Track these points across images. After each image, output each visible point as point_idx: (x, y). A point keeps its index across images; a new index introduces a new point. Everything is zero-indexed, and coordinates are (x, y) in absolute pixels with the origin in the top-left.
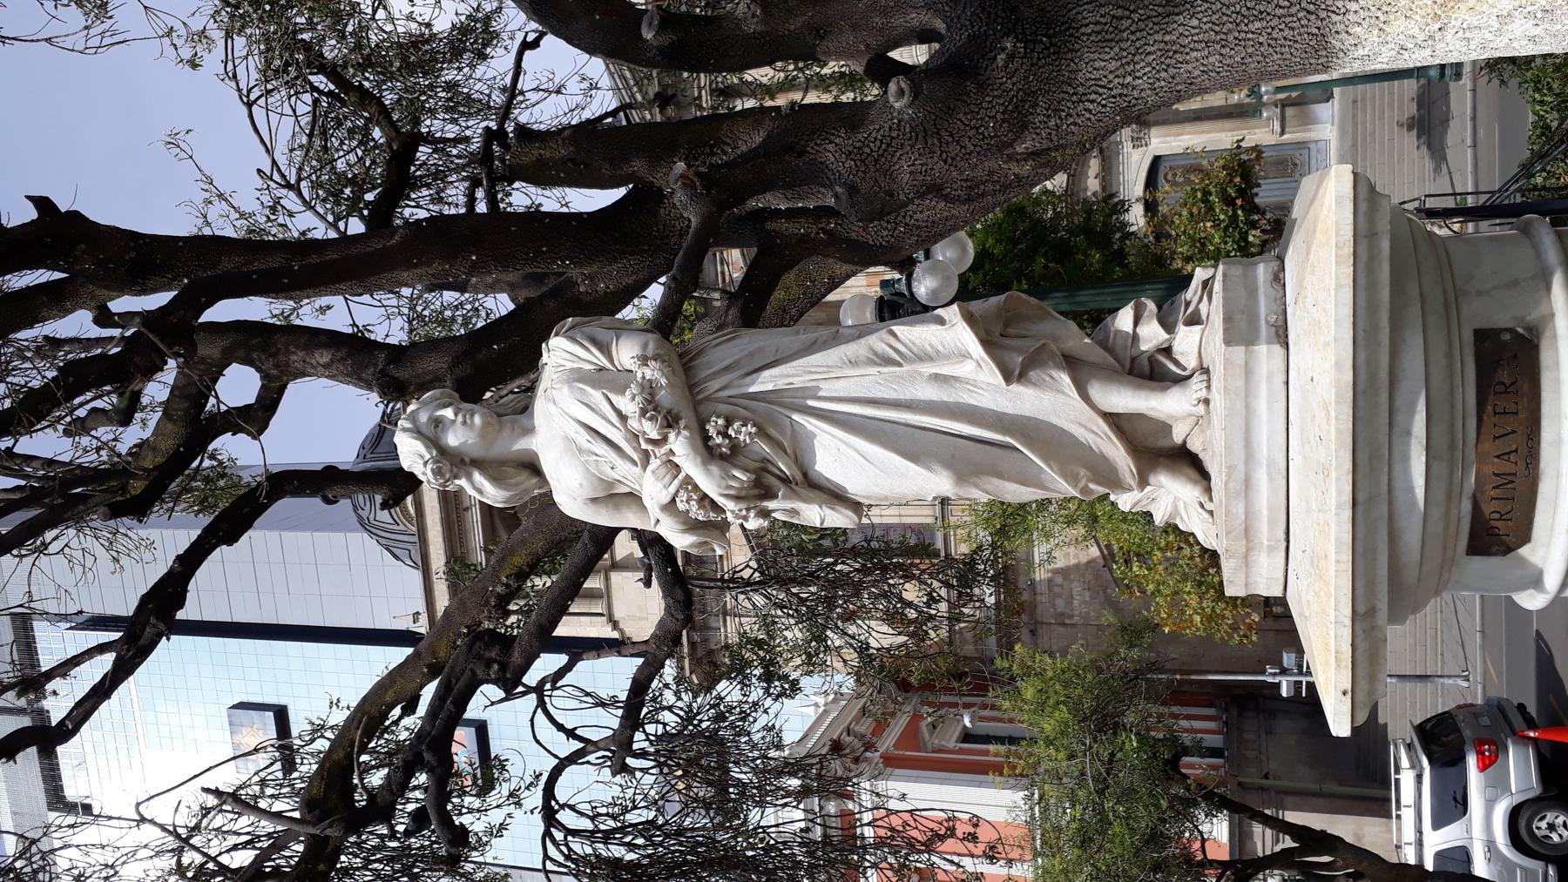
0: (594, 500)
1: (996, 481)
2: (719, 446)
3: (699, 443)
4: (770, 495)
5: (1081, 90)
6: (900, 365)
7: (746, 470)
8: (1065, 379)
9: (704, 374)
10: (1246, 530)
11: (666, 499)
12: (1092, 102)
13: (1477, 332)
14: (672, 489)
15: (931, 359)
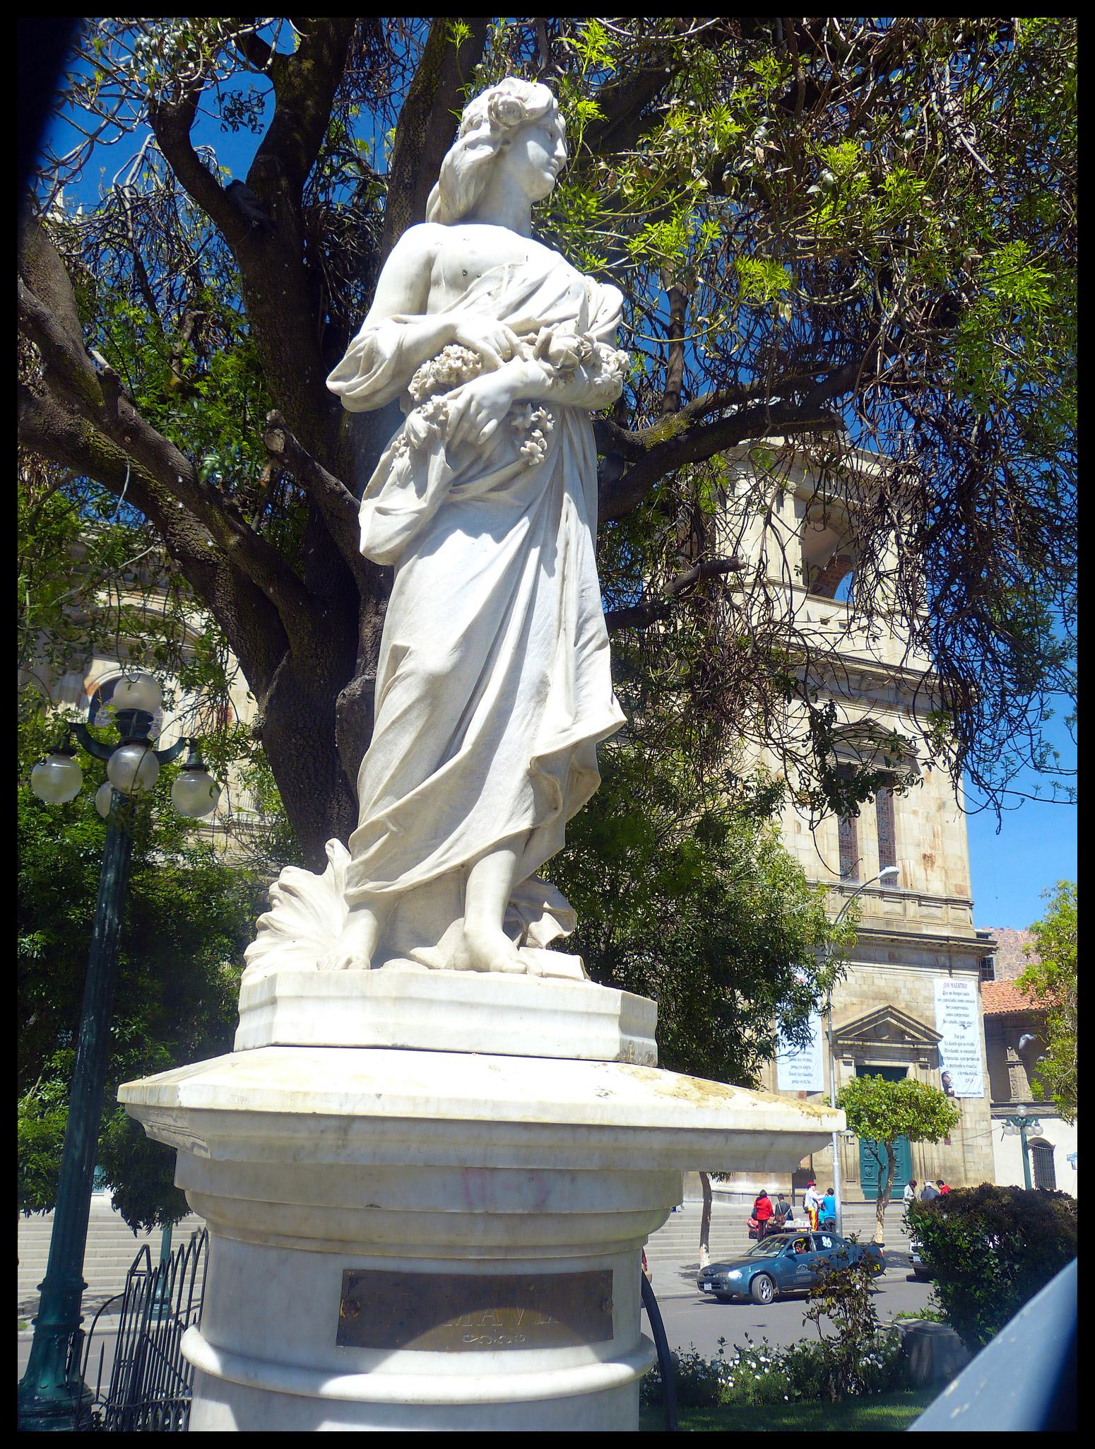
0: (429, 263)
1: (420, 723)
2: (525, 416)
3: (533, 393)
4: (450, 456)
6: (575, 645)
10: (411, 999)
13: (609, 1273)
14: (480, 344)
15: (577, 679)
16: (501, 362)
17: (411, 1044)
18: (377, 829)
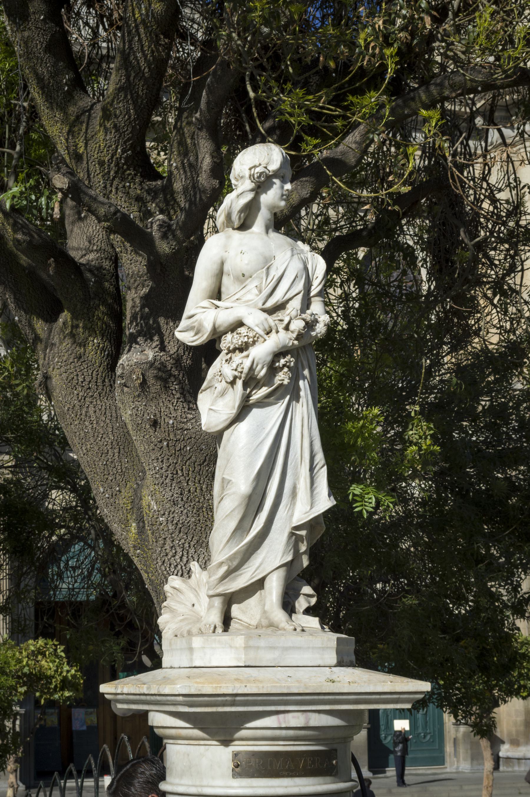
0: (222, 263)
5: (192, 551)
7: (265, 375)
8: (289, 558)
9: (308, 353)
11: (245, 321)
12: (181, 558)
13: (336, 750)
14: (257, 329)
16: (266, 337)
17: (252, 665)
18: (221, 564)
